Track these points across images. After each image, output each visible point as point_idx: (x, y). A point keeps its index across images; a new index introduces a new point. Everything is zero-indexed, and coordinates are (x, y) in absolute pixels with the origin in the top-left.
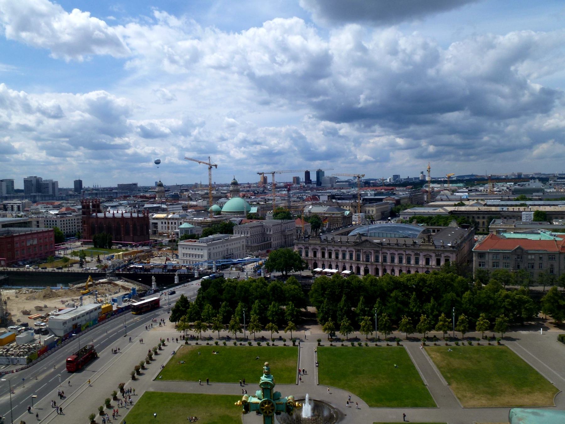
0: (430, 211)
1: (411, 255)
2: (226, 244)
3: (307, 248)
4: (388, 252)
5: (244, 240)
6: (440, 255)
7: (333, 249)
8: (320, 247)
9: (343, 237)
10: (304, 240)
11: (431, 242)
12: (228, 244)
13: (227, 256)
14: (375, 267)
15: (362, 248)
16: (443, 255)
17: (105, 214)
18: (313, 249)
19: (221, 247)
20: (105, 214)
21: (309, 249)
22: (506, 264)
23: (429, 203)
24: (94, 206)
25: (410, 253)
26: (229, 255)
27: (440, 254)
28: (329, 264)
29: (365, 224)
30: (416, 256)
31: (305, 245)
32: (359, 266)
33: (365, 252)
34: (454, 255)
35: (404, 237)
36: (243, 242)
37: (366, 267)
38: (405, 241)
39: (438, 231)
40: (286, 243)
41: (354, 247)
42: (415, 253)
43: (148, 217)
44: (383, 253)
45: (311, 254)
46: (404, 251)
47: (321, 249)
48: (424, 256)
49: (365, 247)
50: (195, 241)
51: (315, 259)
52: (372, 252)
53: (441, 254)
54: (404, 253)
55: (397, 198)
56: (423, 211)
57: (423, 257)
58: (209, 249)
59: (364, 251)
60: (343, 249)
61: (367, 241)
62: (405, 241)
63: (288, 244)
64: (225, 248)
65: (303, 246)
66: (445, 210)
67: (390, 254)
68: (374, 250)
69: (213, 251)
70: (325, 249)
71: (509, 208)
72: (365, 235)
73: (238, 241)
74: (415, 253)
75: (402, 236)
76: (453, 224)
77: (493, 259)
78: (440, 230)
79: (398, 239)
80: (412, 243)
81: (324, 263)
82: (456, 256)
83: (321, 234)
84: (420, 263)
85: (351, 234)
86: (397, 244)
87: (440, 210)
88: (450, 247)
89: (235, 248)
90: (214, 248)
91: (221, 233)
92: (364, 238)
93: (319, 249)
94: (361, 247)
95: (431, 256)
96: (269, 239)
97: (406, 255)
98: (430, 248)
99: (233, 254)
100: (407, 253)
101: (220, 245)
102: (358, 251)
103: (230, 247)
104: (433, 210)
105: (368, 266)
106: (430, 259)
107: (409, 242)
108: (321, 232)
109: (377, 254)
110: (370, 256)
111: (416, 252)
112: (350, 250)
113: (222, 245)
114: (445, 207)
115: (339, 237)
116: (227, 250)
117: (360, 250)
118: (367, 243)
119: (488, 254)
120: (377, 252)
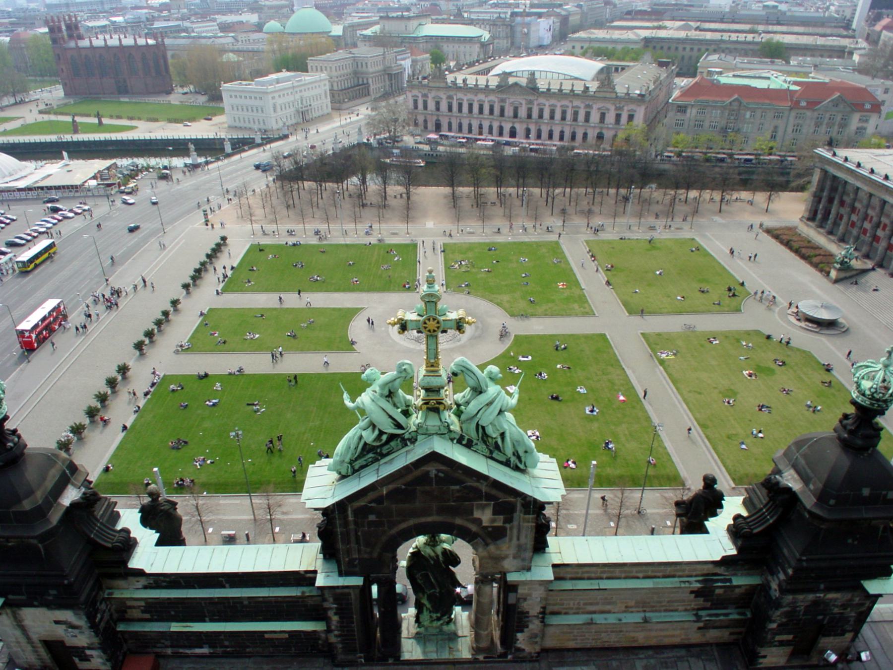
3: (425, 96)
6: (621, 109)
9: (479, 77)
15: (507, 96)
16: (626, 108)
18: (434, 98)
21: (428, 97)
28: (458, 121)
32: (503, 124)
39: (623, 69)
45: (431, 105)
46: (571, 102)
48: (599, 109)
51: (438, 113)
52: (524, 102)
55: (563, 13)
59: (512, 100)
61: (516, 84)
70: (453, 99)
87: (630, 35)
88: (639, 95)
92: (511, 80)
93: (444, 97)
95: (608, 110)
98: (608, 95)
100: (574, 104)
108: (446, 70)
111: (587, 103)
114: (636, 31)
115: (475, 77)
117: (505, 99)
120: (530, 102)
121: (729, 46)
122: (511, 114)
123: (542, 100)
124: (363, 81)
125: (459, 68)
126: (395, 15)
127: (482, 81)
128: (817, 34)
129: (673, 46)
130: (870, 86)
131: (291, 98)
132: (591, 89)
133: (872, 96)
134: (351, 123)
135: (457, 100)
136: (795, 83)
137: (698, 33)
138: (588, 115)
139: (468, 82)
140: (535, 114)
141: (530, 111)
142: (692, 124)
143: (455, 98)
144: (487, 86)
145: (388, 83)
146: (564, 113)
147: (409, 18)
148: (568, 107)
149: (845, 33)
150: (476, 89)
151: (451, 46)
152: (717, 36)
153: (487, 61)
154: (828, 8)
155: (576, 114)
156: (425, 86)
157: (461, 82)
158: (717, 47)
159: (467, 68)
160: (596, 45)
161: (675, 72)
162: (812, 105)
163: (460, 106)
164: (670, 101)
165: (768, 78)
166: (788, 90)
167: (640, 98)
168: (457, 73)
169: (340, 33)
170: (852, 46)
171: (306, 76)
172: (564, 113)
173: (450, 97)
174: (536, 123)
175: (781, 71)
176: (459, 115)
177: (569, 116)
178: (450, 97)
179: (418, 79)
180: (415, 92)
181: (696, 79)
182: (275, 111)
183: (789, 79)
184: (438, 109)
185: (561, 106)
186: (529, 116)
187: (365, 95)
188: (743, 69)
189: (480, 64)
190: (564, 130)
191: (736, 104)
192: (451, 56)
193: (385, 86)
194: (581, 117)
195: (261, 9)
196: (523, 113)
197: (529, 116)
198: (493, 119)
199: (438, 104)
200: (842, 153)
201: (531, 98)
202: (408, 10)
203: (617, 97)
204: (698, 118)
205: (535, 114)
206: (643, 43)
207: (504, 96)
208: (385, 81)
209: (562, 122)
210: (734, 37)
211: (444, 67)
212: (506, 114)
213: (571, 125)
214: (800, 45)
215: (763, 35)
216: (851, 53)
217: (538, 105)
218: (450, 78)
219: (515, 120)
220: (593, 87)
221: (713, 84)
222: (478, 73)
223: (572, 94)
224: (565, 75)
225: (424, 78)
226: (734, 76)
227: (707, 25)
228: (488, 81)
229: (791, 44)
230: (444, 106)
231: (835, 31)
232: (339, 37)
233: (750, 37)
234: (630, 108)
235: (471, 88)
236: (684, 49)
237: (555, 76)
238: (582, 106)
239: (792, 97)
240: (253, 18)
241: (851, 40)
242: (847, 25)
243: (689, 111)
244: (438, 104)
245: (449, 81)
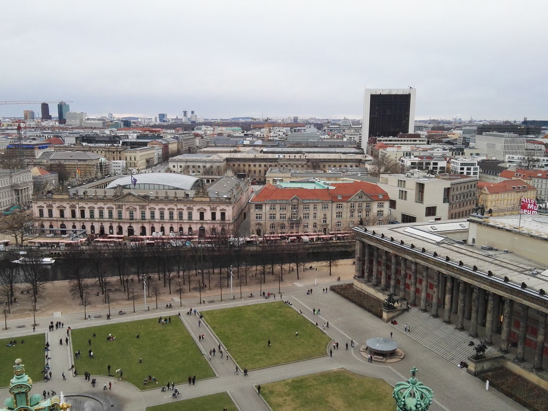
0: (203, 158)
1: (183, 209)
3: (50, 206)
4: (157, 207)
7: (87, 206)
8: (67, 204)
10: (46, 195)
11: (205, 193)
14: (141, 225)
15: (124, 203)
16: (218, 208)
21: (52, 207)
22: (283, 216)
23: (202, 148)
25: (182, 208)
27: (215, 207)
28: (82, 225)
29: (126, 174)
30: (190, 211)
31: (47, 202)
32: (121, 225)
33: (128, 208)
34: (231, 207)
35: (174, 189)
37: (130, 226)
38: (176, 193)
40: (19, 200)
41: (114, 203)
42: (188, 208)
44: (150, 209)
45: (56, 213)
46: (175, 205)
47: (70, 207)
48: (198, 210)
49: (127, 202)
52: (138, 207)
53: (216, 207)
54: (175, 208)
56: (195, 158)
57: (197, 211)
59: (127, 207)
60: (99, 206)
62: (176, 193)
63: (22, 202)
65: (44, 203)
66: (220, 157)
67: (159, 209)
68: (139, 205)
70: (76, 207)
71: (290, 155)
72: (126, 187)
74: (188, 208)
75: (173, 188)
76: (230, 173)
77: (270, 211)
78: (215, 180)
79: (167, 191)
81: (75, 225)
82: (233, 208)
83: (69, 187)
84: (194, 218)
85: (109, 186)
86: (167, 197)
87: (215, 157)
88: (226, 198)
92: (125, 191)
93: (68, 206)
94: (122, 202)
95: (205, 210)
97: (177, 209)
100: (178, 208)
102: (120, 207)
104: (206, 157)
105: (132, 225)
106: (205, 214)
107: (181, 195)
109: (143, 210)
110: (134, 212)
111: (189, 206)
112: (109, 206)
117: (122, 205)
118: (130, 197)
119: (265, 205)
120: (143, 207)
122: (128, 217)
123: (152, 205)
127: (100, 192)
132: (190, 196)
135: (79, 208)
137: (262, 154)
139: (88, 194)
141: (143, 214)
142: (268, 216)
143: (77, 206)
146: (171, 214)
148: (174, 209)
153: (104, 178)
155: (181, 215)
156: (49, 198)
157: (82, 194)
159: (87, 183)
161: (250, 181)
164: (250, 201)
167: (227, 200)
168: (79, 187)
172: (171, 214)
173: (73, 206)
174: (150, 222)
176: (82, 219)
178: (73, 206)
180: (41, 203)
184: (62, 215)
185: (169, 209)
186: (143, 218)
189: (98, 180)
190: (173, 226)
194: (185, 216)
196: (137, 215)
197: (143, 218)
198: (112, 221)
201: (144, 204)
203: (211, 201)
206: (225, 162)
207: (121, 204)
209: (171, 221)
212: (123, 217)
213: (178, 223)
217: (150, 209)
219: (132, 221)
220: (192, 194)
223: (176, 200)
224: (169, 186)
230: (68, 213)
234: (221, 208)
235: (91, 198)
237: (162, 187)
238: (185, 208)
243: (264, 207)
245: (71, 193)
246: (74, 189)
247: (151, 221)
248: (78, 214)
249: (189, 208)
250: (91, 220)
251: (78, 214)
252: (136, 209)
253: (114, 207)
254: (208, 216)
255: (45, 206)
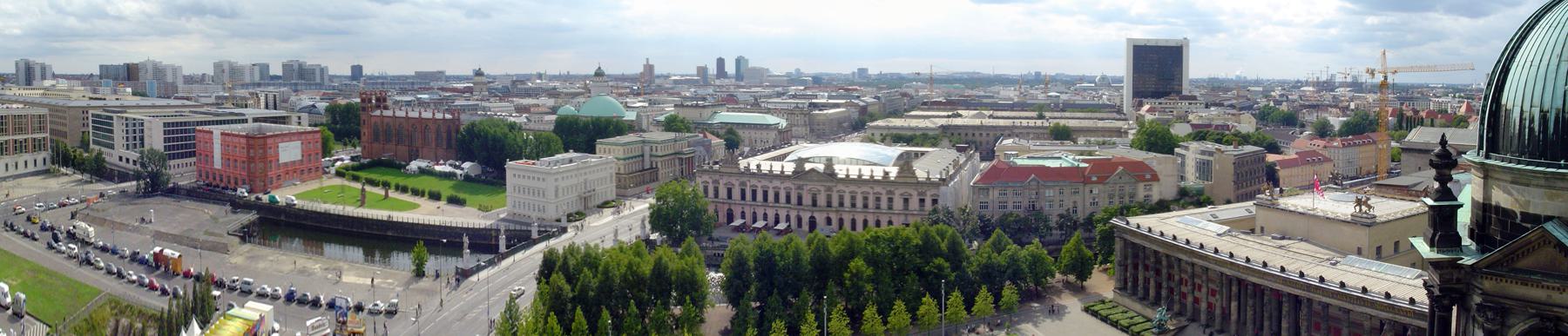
2: (583, 171)
5: (613, 165)
7: (759, 185)
9: (774, 163)
12: (587, 171)
13: (585, 193)
15: (805, 183)
16: (929, 193)
17: (394, 112)
18: (725, 184)
19: (576, 175)
20: (394, 112)
24: (378, 100)
26: (589, 192)
28: (752, 211)
30: (890, 196)
32: (802, 214)
33: (810, 190)
36: (611, 168)
40: (682, 172)
43: (459, 119)
45: (723, 193)
46: (872, 188)
47: (740, 185)
48: (902, 195)
50: (534, 164)
51: (729, 201)
52: (822, 189)
54: (871, 191)
58: (556, 180)
59: (809, 187)
64: (582, 179)
69: (562, 184)
70: (746, 186)
73: (604, 167)
80: (882, 174)
85: (789, 158)
89: (598, 180)
90: (563, 178)
91: (575, 151)
92: (808, 166)
93: (737, 183)
95: (911, 195)
96: (654, 166)
98: (908, 180)
99: (594, 190)
101: (573, 174)
103: (590, 177)
108: (740, 155)
111: (888, 189)
113: (576, 172)
115: (769, 162)
116: (585, 183)
120: (829, 189)
121: (1022, 131)
122: (810, 203)
123: (841, 187)
124: (652, 165)
125: (754, 153)
126: (689, 104)
127: (777, 167)
128: (1096, 119)
129: (970, 132)
130: (1147, 159)
131: (574, 181)
132: (891, 175)
133: (1151, 170)
134: (635, 213)
135: (751, 186)
136: (1084, 161)
137: (991, 120)
138: (890, 200)
140: (835, 203)
141: (829, 198)
144: (782, 172)
145: (678, 168)
147: (704, 107)
148: (869, 193)
149: (1119, 117)
150: (771, 176)
151: (747, 132)
152: (1008, 123)
154: (1101, 97)
157: (755, 167)
158: (1010, 132)
160: (895, 132)
162: (1101, 181)
163: (754, 193)
165: (1060, 158)
166: (1078, 167)
169: (634, 118)
170: (1126, 127)
171: (593, 158)
173: (743, 184)
174: (837, 211)
175: (1071, 151)
177: (871, 203)
178: (743, 184)
179: (709, 164)
180: (706, 178)
181: (994, 162)
182: (556, 195)
183: (1077, 157)
184: (730, 196)
186: (829, 205)
187: (654, 181)
188: (1037, 151)
189: (776, 149)
191: (1034, 183)
192: (747, 142)
193: (675, 171)
194: (884, 204)
195: (559, 95)
196: (822, 201)
197: (829, 205)
199: (730, 191)
200: (1134, 220)
202: (704, 99)
203: (919, 183)
204: (1001, 200)
205: (835, 203)
206: (941, 129)
207: (801, 183)
208: (675, 165)
210: (1025, 123)
211: (737, 152)
212: (804, 202)
214: (1082, 127)
215: (1050, 120)
216: (1126, 133)
217: (838, 191)
218: (743, 163)
219: (814, 209)
221: (1011, 167)
222: (774, 159)
225: (716, 163)
226: (1028, 157)
227: (999, 114)
228: (783, 167)
229: (1075, 127)
230: (736, 194)
231: (1110, 115)
232: (633, 121)
233: (1039, 122)
234: (932, 193)
235: (765, 174)
236: (981, 134)
238: (884, 192)
239: (1083, 173)
240: (551, 102)
241: (1124, 122)
242: (1120, 111)
244: (730, 191)
245: (742, 167)
246: (746, 161)
247: (839, 209)
248: (749, 196)
249: (890, 192)
250: (765, 204)
251: (749, 196)
252: (820, 191)
253: (793, 187)
254: (914, 204)
255: (710, 181)
